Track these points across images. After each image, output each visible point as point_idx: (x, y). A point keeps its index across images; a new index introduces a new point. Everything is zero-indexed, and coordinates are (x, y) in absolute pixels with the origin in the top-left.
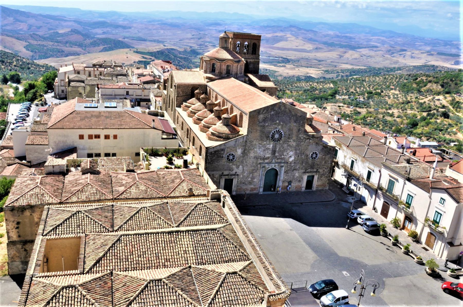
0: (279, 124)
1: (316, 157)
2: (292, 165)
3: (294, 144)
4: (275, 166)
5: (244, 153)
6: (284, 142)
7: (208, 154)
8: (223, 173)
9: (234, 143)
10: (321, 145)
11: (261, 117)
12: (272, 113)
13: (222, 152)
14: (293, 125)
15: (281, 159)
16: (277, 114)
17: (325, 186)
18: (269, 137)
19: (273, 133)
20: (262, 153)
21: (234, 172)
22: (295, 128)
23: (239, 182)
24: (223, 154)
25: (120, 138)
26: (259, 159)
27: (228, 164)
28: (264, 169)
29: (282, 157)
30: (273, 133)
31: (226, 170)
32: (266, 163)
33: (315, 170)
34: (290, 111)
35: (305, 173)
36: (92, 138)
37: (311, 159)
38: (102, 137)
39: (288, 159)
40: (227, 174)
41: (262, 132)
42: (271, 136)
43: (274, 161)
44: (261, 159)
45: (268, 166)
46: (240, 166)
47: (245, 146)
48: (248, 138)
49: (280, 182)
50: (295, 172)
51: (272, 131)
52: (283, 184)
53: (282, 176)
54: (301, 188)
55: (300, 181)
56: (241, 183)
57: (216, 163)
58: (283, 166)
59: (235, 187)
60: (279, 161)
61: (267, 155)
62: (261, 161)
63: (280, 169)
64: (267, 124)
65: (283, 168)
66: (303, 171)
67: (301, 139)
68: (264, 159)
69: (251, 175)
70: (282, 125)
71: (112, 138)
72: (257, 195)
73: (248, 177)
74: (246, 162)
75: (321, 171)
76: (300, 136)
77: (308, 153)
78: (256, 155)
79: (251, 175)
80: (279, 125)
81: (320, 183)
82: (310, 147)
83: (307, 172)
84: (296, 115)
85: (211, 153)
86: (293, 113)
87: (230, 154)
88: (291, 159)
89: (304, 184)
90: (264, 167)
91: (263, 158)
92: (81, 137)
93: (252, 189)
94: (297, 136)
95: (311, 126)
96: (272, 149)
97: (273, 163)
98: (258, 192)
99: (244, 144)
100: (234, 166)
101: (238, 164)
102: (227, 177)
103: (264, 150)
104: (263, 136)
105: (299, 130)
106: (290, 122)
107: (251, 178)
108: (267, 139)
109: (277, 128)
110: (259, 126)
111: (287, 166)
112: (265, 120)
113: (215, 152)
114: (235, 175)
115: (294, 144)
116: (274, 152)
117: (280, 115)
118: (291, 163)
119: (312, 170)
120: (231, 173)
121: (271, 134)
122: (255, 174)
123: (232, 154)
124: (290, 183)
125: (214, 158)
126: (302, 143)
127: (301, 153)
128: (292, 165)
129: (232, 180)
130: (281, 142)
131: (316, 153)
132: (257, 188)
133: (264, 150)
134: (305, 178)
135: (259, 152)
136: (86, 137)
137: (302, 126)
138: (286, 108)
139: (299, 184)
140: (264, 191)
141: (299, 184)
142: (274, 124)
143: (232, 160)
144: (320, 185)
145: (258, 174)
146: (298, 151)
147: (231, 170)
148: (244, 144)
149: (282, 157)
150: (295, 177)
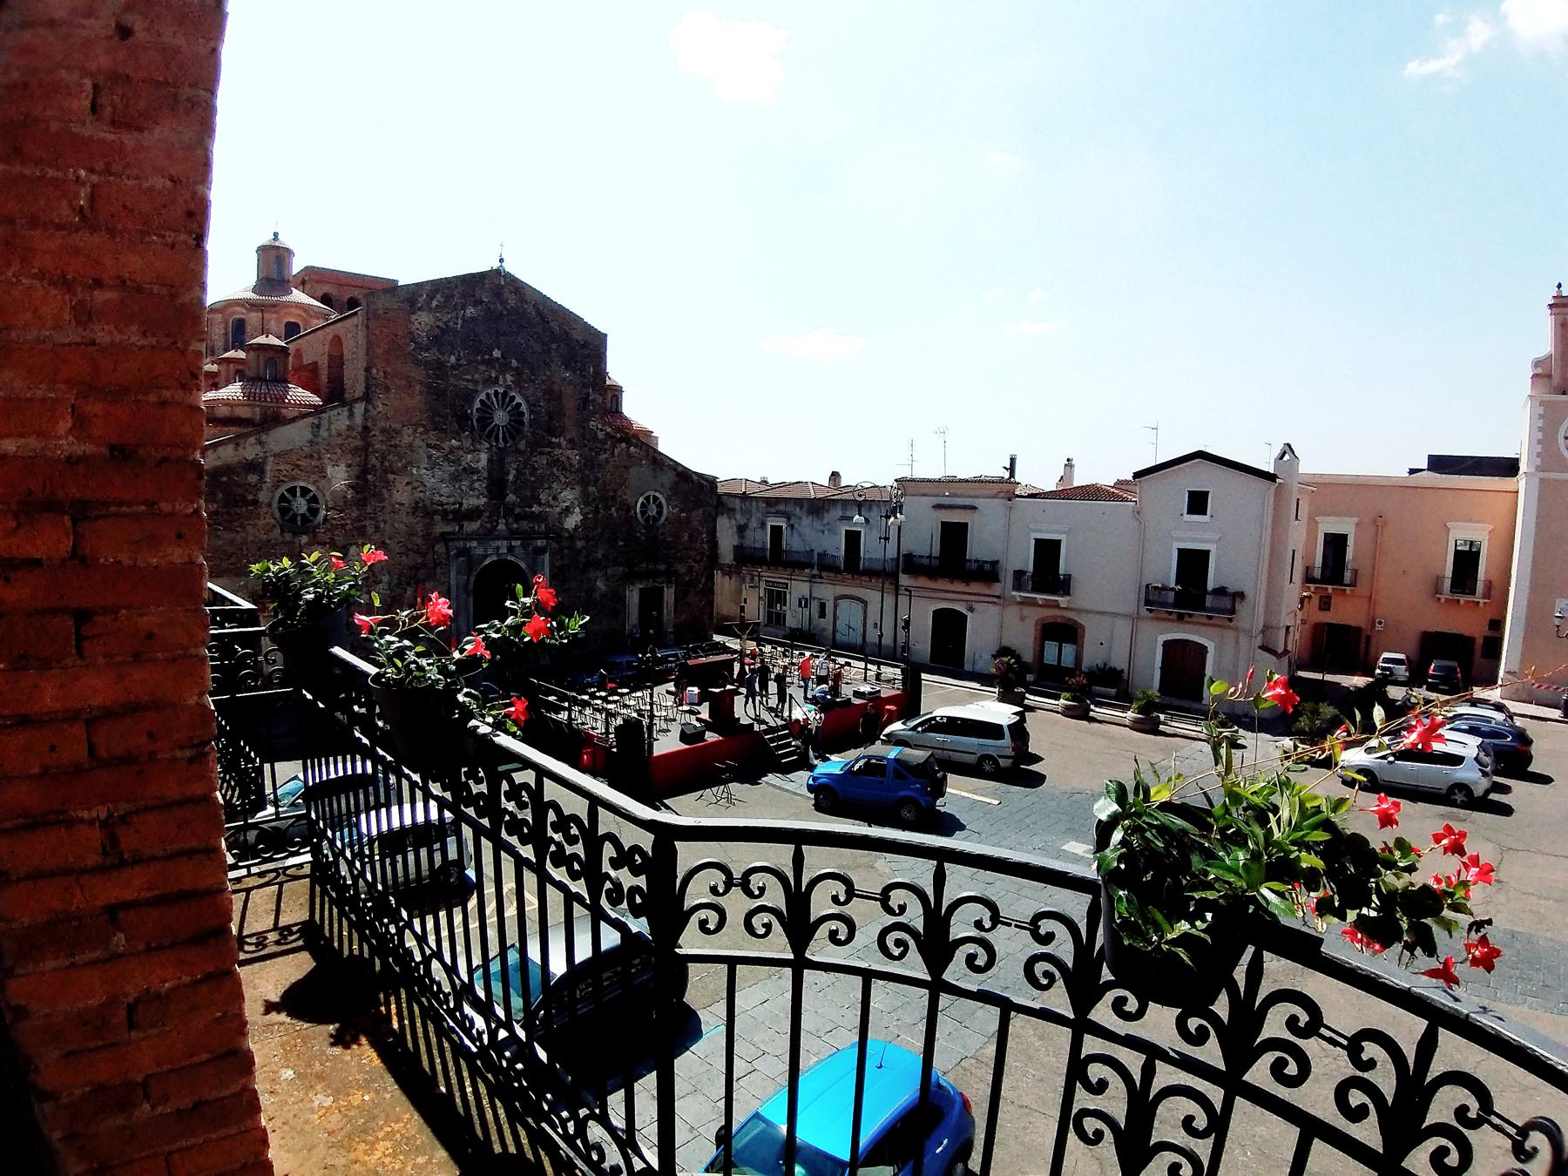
0: (504, 367)
1: (660, 513)
2: (579, 544)
3: (575, 457)
4: (511, 549)
5: (366, 487)
6: (536, 445)
9: (308, 435)
11: (423, 321)
13: (253, 478)
15: (533, 517)
18: (468, 417)
19: (481, 401)
24: (257, 487)
26: (438, 518)
27: (288, 537)
30: (481, 401)
33: (663, 567)
35: (629, 578)
41: (436, 393)
42: (476, 415)
43: (501, 527)
45: (480, 551)
48: (373, 412)
51: (476, 391)
57: (228, 536)
58: (542, 551)
60: (525, 525)
61: (474, 501)
63: (534, 560)
68: (461, 516)
70: (518, 373)
75: (682, 569)
77: (628, 498)
78: (418, 495)
80: (503, 372)
82: (633, 472)
87: (292, 491)
88: (573, 521)
91: (454, 512)
94: (582, 424)
96: (490, 471)
97: (497, 538)
99: (359, 443)
103: (455, 478)
109: (497, 379)
110: (417, 363)
112: (440, 338)
115: (575, 457)
116: (496, 487)
118: (572, 538)
121: (477, 405)
123: (305, 491)
126: (604, 456)
128: (579, 544)
130: (522, 445)
134: (633, 597)
135: (431, 482)
142: (483, 362)
146: (591, 489)
148: (359, 443)
150: (597, 596)
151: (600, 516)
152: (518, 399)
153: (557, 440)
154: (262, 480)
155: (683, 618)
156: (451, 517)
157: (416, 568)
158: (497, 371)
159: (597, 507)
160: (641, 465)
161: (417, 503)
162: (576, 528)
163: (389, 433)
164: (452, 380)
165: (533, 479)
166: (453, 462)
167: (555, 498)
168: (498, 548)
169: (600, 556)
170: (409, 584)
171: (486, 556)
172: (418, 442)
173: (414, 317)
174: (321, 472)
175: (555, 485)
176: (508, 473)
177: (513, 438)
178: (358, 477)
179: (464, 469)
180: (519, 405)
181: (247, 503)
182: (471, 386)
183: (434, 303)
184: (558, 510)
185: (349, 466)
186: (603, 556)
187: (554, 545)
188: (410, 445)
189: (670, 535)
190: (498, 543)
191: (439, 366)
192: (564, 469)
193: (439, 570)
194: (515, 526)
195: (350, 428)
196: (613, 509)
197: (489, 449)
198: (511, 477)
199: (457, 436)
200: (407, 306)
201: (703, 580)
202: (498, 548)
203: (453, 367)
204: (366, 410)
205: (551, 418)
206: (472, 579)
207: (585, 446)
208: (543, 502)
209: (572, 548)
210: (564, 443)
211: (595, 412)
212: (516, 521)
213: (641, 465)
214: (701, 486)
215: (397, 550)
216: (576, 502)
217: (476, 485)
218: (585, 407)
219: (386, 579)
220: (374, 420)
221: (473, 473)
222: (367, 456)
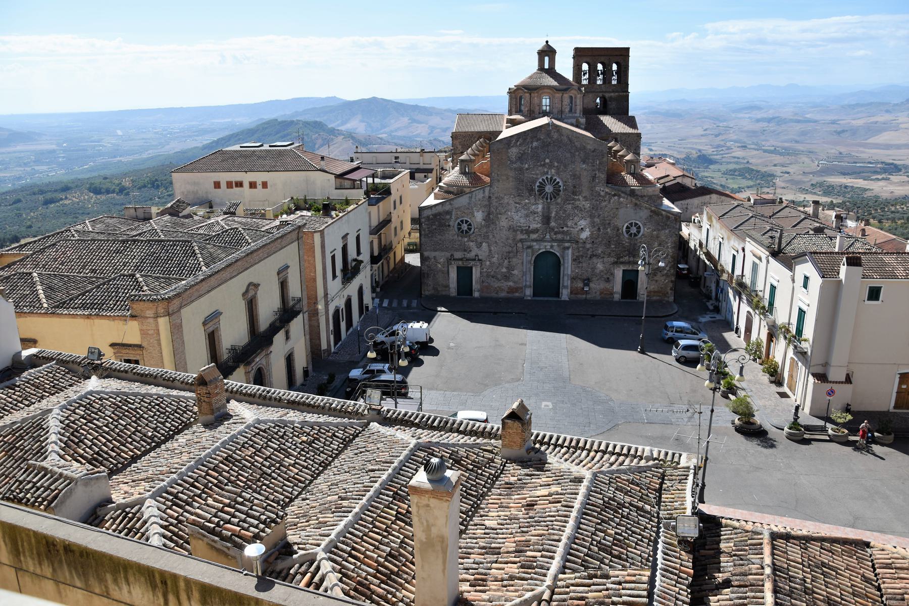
0: (551, 166)
1: (639, 232)
2: (588, 246)
3: (587, 205)
4: (552, 247)
5: (490, 219)
6: (566, 200)
7: (423, 220)
8: (452, 255)
10: (646, 208)
11: (514, 151)
12: (535, 144)
13: (448, 217)
14: (582, 168)
15: (563, 233)
16: (545, 146)
17: (665, 294)
20: (522, 221)
21: (472, 255)
22: (585, 173)
23: (485, 274)
25: (271, 186)
26: (519, 232)
27: (460, 238)
28: (529, 250)
29: (565, 229)
31: (457, 250)
32: (533, 240)
34: (570, 140)
36: (232, 188)
37: (626, 236)
38: (246, 184)
39: (578, 235)
40: (460, 257)
42: (537, 188)
43: (548, 237)
44: (522, 231)
45: (537, 247)
46: (484, 244)
47: (489, 206)
48: (493, 191)
49: (566, 278)
50: (595, 260)
51: (538, 179)
52: (572, 282)
53: (568, 268)
54: (612, 294)
55: (608, 280)
56: (488, 276)
57: (439, 237)
58: (568, 248)
59: (477, 282)
60: (559, 236)
61: (534, 226)
63: (563, 252)
64: (527, 166)
65: (570, 251)
67: (599, 195)
68: (528, 232)
69: (506, 261)
70: (558, 168)
71: (259, 187)
72: (521, 300)
74: (494, 236)
76: (597, 189)
77: (620, 225)
78: (510, 223)
79: (506, 261)
81: (652, 287)
82: (622, 211)
83: (622, 263)
84: (585, 148)
85: (428, 217)
87: (462, 221)
88: (585, 235)
89: (618, 287)
90: (530, 247)
92: (217, 185)
93: (511, 290)
94: (592, 189)
95: (633, 175)
97: (546, 241)
98: (522, 295)
100: (471, 244)
101: (479, 240)
102: (460, 263)
103: (527, 216)
104: (521, 187)
105: (594, 178)
106: (573, 162)
107: (507, 268)
109: (547, 173)
110: (511, 169)
111: (578, 248)
112: (521, 158)
113: (435, 215)
114: (474, 260)
115: (587, 205)
116: (546, 219)
119: (631, 259)
120: (469, 256)
121: (538, 184)
122: (514, 260)
123: (467, 222)
124: (587, 281)
125: (434, 227)
126: (604, 204)
129: (471, 268)
130: (559, 200)
131: (636, 224)
132: (521, 288)
134: (618, 274)
135: (516, 218)
136: (223, 185)
138: (561, 135)
140: (535, 295)
141: (608, 286)
142: (541, 165)
143: (466, 232)
144: (655, 292)
145: (520, 261)
146: (596, 220)
147: (467, 250)
149: (565, 229)
150: (597, 271)
152: (558, 180)
154: (451, 217)
155: (652, 287)
157: (509, 252)
159: (599, 229)
160: (627, 208)
162: (586, 238)
164: (526, 175)
167: (576, 224)
168: (546, 246)
169: (600, 252)
171: (540, 249)
172: (511, 202)
174: (473, 214)
175: (576, 218)
181: (446, 226)
182: (535, 176)
184: (577, 229)
187: (574, 245)
190: (546, 244)
191: (521, 170)
192: (581, 210)
193: (518, 254)
195: (484, 197)
196: (609, 230)
197: (543, 203)
198: (553, 215)
199: (528, 198)
202: (546, 246)
205: (575, 187)
206: (533, 259)
209: (583, 247)
210: (581, 198)
211: (599, 182)
212: (555, 234)
213: (627, 208)
214: (668, 218)
215: (502, 245)
217: (537, 219)
218: (593, 180)
219: (496, 256)
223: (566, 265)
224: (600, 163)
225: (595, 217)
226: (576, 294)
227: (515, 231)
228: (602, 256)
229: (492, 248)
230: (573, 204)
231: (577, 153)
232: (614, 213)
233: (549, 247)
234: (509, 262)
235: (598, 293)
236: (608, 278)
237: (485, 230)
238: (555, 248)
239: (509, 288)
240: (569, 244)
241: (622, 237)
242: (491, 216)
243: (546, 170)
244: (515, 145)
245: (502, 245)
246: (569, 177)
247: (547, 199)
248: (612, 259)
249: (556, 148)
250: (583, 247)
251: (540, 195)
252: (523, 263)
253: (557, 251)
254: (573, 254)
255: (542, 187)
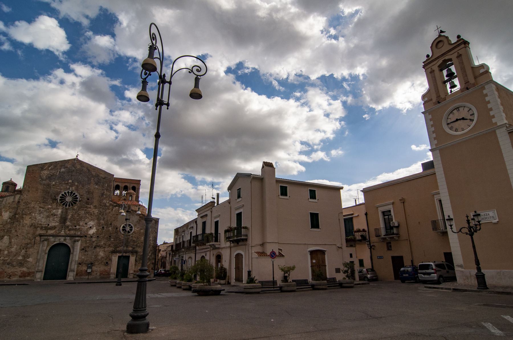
0: (72, 185)
1: (131, 230)
2: (94, 239)
3: (96, 211)
4: (65, 240)
6: (80, 208)
11: (45, 173)
14: (93, 187)
15: (76, 230)
19: (62, 195)
20: (43, 220)
26: (39, 229)
28: (46, 242)
29: (78, 227)
30: (62, 195)
33: (131, 249)
34: (88, 169)
35: (114, 252)
39: (87, 231)
42: (59, 198)
44: (41, 228)
46: (6, 237)
49: (73, 263)
50: (98, 249)
51: (61, 192)
52: (78, 267)
53: (76, 255)
54: (109, 274)
55: (107, 264)
58: (78, 241)
60: (72, 232)
61: (52, 224)
62: (42, 232)
63: (74, 244)
64: (54, 183)
65: (80, 243)
66: (111, 249)
67: (105, 206)
68: (47, 228)
69: (23, 251)
70: (77, 186)
73: (17, 254)
74: (16, 231)
76: (105, 201)
77: (118, 225)
80: (72, 186)
84: (98, 176)
86: (94, 173)
88: (91, 232)
89: (114, 268)
93: (24, 275)
96: (61, 215)
99: (16, 206)
103: (48, 217)
106: (89, 184)
107: (23, 256)
108: (53, 202)
110: (41, 184)
111: (86, 241)
112: (50, 177)
115: (96, 211)
116: (63, 220)
117: (73, 174)
121: (61, 195)
122: (31, 250)
124: (91, 265)
126: (108, 211)
127: (107, 224)
128: (94, 239)
130: (75, 207)
131: (130, 225)
132: (33, 273)
133: (48, 217)
134: (115, 259)
135: (38, 217)
137: (107, 190)
138: (83, 166)
139: (106, 268)
141: (106, 268)
142: (65, 183)
145: (36, 251)
146: (102, 222)
148: (16, 206)
149: (78, 227)
150: (100, 258)
151: (104, 230)
152: (76, 194)
153: (89, 206)
156: (44, 228)
157: (27, 244)
158: (69, 186)
159: (103, 228)
161: (32, 224)
162: (93, 234)
163: (26, 203)
164: (52, 189)
165: (78, 218)
166: (48, 212)
167: (86, 224)
169: (102, 243)
170: (23, 249)
171: (55, 241)
173: (42, 172)
175: (86, 220)
176: (68, 216)
177: (72, 205)
178: (13, 216)
179: (52, 214)
180: (77, 195)
182: (59, 190)
183: (50, 168)
184: (86, 228)
185: (10, 212)
186: (104, 244)
188: (33, 207)
189: (135, 238)
191: (49, 185)
192: (91, 215)
193: (35, 245)
194: (68, 232)
195: (14, 201)
196: (110, 228)
198: (69, 217)
199: (51, 204)
200: (40, 169)
201: (150, 254)
203: (54, 185)
204: (20, 197)
205: (88, 199)
206: (48, 249)
207: (100, 208)
208: (81, 225)
211: (106, 198)
215: (22, 238)
216: (95, 226)
219: (15, 247)
220: (22, 200)
221: (55, 215)
222: (17, 210)
223: (75, 253)
224: (108, 186)
225: (101, 219)
226: (81, 275)
227: (36, 227)
228: (104, 246)
229: (13, 240)
230: (86, 210)
231: (92, 179)
232: (115, 217)
233: (63, 240)
234: (26, 252)
235: (98, 274)
236: (107, 263)
237: (9, 226)
238: (67, 240)
239: (22, 273)
240: (79, 238)
241: (119, 233)
242: (17, 216)
243: (68, 187)
244: (47, 169)
245: (22, 238)
246: (84, 192)
247: (66, 206)
248: (111, 249)
249: (78, 174)
250: (90, 240)
251: (61, 203)
252: (38, 252)
253: (68, 242)
254: (81, 245)
255: (63, 198)
